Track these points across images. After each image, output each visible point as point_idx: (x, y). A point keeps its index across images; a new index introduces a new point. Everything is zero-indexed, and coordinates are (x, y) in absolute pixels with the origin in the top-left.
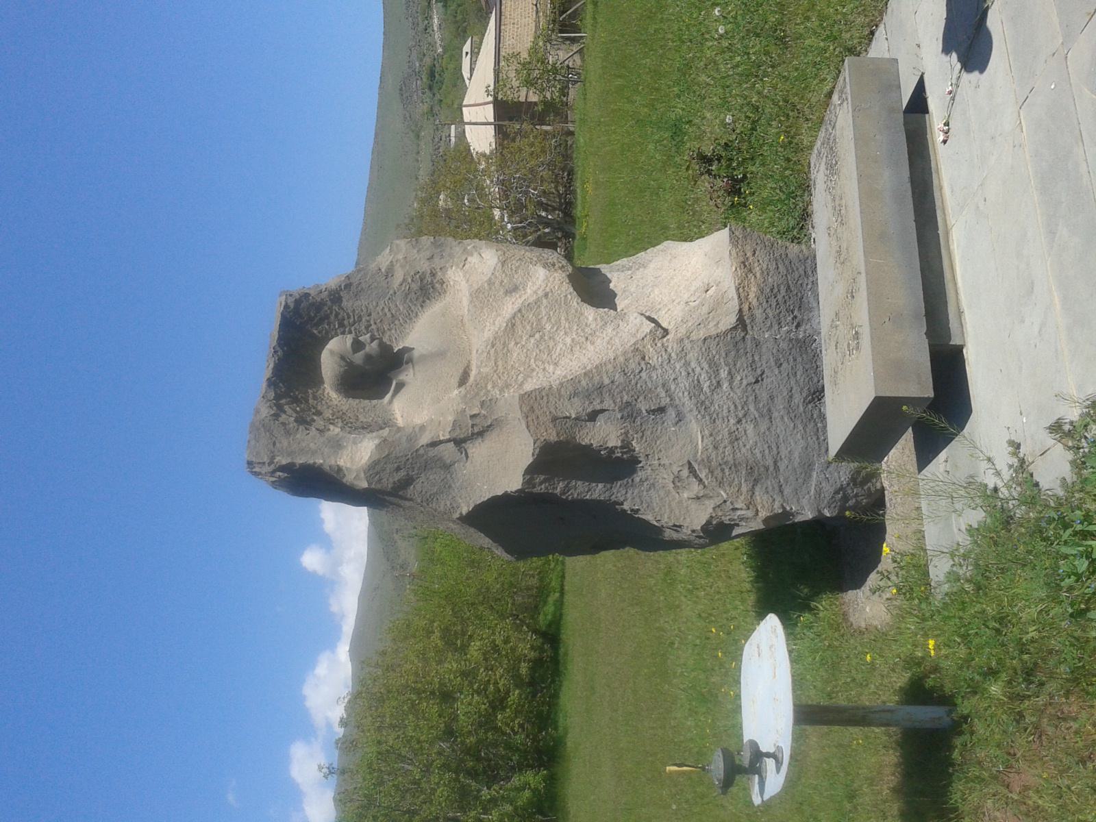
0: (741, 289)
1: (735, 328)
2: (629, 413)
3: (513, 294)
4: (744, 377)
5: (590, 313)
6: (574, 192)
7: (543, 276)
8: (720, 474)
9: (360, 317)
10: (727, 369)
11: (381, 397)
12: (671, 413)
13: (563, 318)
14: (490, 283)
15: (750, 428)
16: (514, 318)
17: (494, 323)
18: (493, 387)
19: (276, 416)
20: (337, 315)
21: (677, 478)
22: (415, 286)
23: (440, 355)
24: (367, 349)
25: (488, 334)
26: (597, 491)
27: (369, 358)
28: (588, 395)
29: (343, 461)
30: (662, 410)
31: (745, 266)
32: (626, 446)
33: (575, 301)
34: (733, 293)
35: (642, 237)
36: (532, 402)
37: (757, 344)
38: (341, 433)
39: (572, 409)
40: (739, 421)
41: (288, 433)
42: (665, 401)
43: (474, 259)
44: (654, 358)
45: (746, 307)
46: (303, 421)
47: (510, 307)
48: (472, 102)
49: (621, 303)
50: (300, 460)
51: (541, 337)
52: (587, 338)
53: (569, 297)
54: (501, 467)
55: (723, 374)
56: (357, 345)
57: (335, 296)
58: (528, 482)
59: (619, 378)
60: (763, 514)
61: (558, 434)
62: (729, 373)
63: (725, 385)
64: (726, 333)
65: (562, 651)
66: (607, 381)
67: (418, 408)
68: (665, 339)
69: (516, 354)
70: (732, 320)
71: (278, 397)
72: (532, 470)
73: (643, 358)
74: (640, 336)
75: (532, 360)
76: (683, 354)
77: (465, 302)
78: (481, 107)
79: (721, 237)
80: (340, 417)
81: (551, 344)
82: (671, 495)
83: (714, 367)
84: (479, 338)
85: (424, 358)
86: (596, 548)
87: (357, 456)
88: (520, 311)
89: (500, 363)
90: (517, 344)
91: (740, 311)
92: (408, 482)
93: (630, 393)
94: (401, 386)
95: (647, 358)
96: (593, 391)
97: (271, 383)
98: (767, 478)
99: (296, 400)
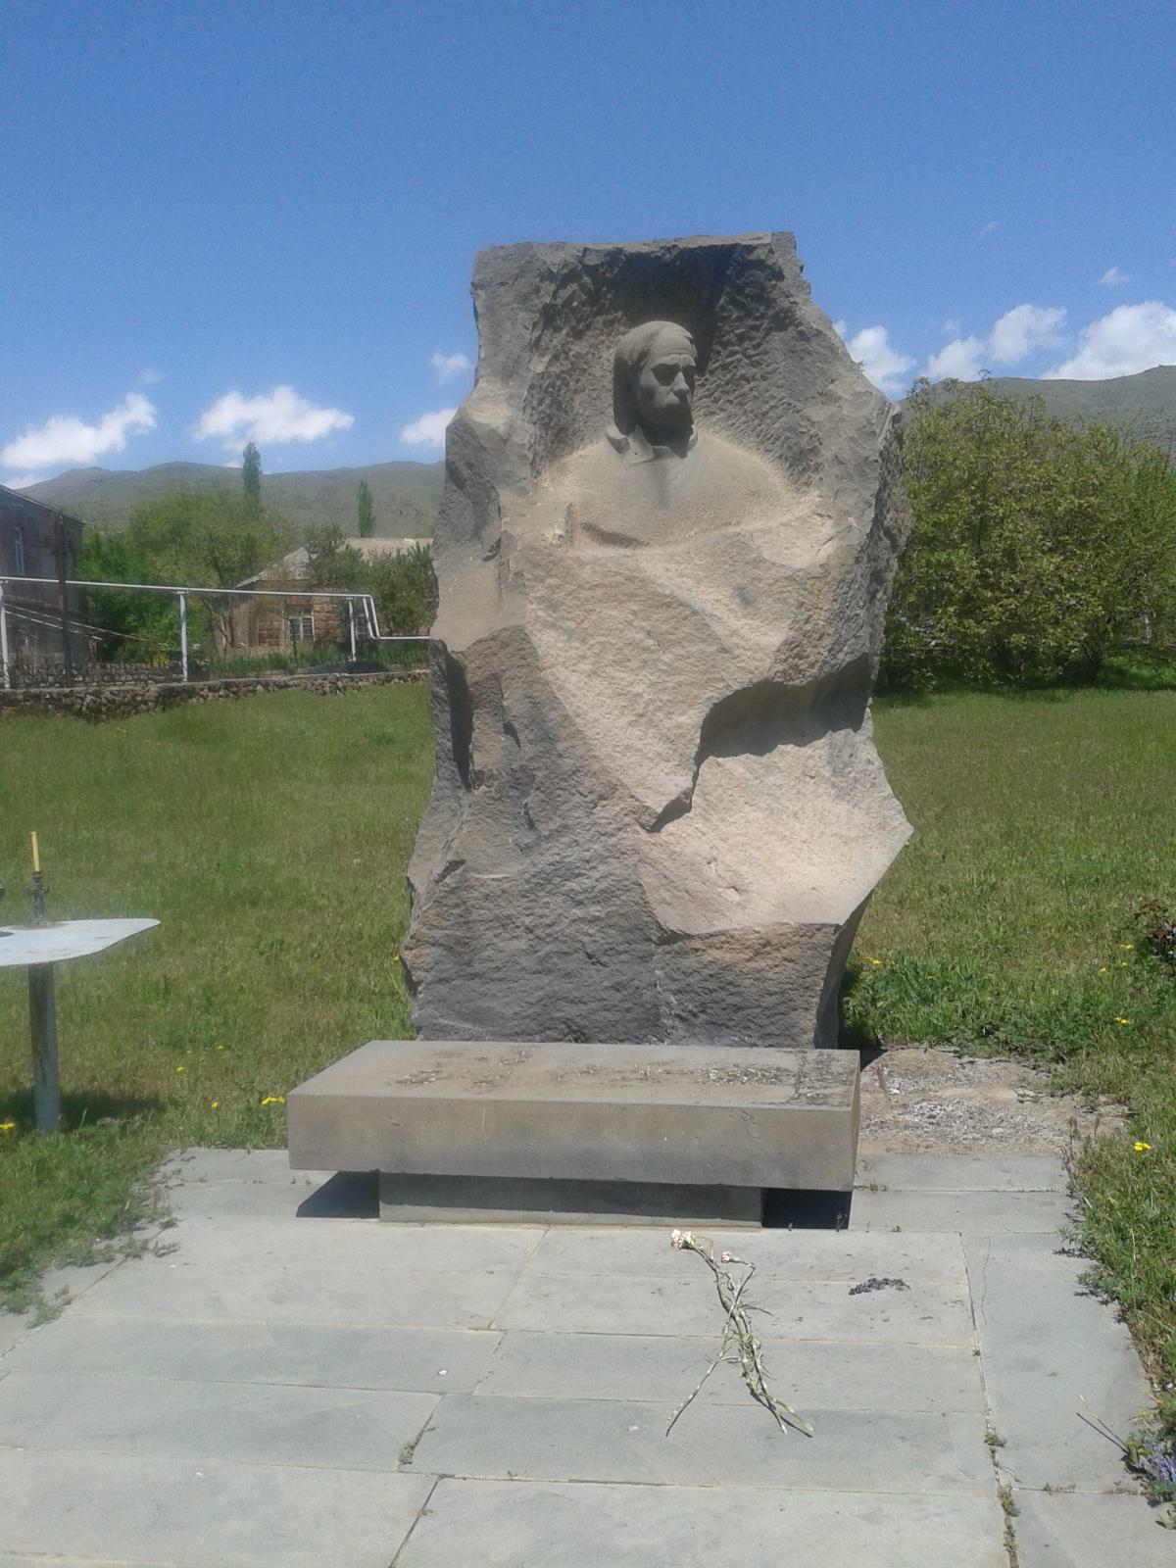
0: (724, 939)
1: (661, 928)
2: (520, 780)
3: (738, 600)
4: (594, 938)
5: (691, 719)
8: (450, 903)
9: (757, 364)
10: (602, 915)
12: (528, 838)
13: (682, 678)
14: (758, 562)
15: (521, 944)
16: (681, 605)
18: (550, 587)
19: (550, 276)
20: (756, 328)
22: (804, 441)
24: (663, 389)
27: (650, 393)
28: (536, 721)
30: (531, 825)
31: (764, 946)
33: (714, 694)
34: (720, 925)
37: (644, 958)
38: (531, 375)
39: (513, 700)
40: (529, 930)
41: (524, 299)
42: (544, 829)
44: (604, 813)
45: (697, 944)
46: (549, 317)
51: (646, 649)
52: (641, 715)
53: (722, 685)
55: (594, 910)
57: (784, 320)
59: (568, 763)
61: (476, 683)
62: (597, 919)
63: (578, 912)
64: (650, 914)
65: (1060, 693)
66: (560, 747)
68: (639, 828)
69: (614, 614)
70: (673, 921)
71: (592, 271)
73: (602, 797)
74: (640, 792)
75: (603, 639)
81: (634, 664)
83: (605, 897)
88: (695, 613)
89: (598, 592)
90: (634, 613)
91: (690, 937)
95: (604, 802)
96: (544, 726)
97: (614, 256)
98: (455, 963)
99: (594, 298)
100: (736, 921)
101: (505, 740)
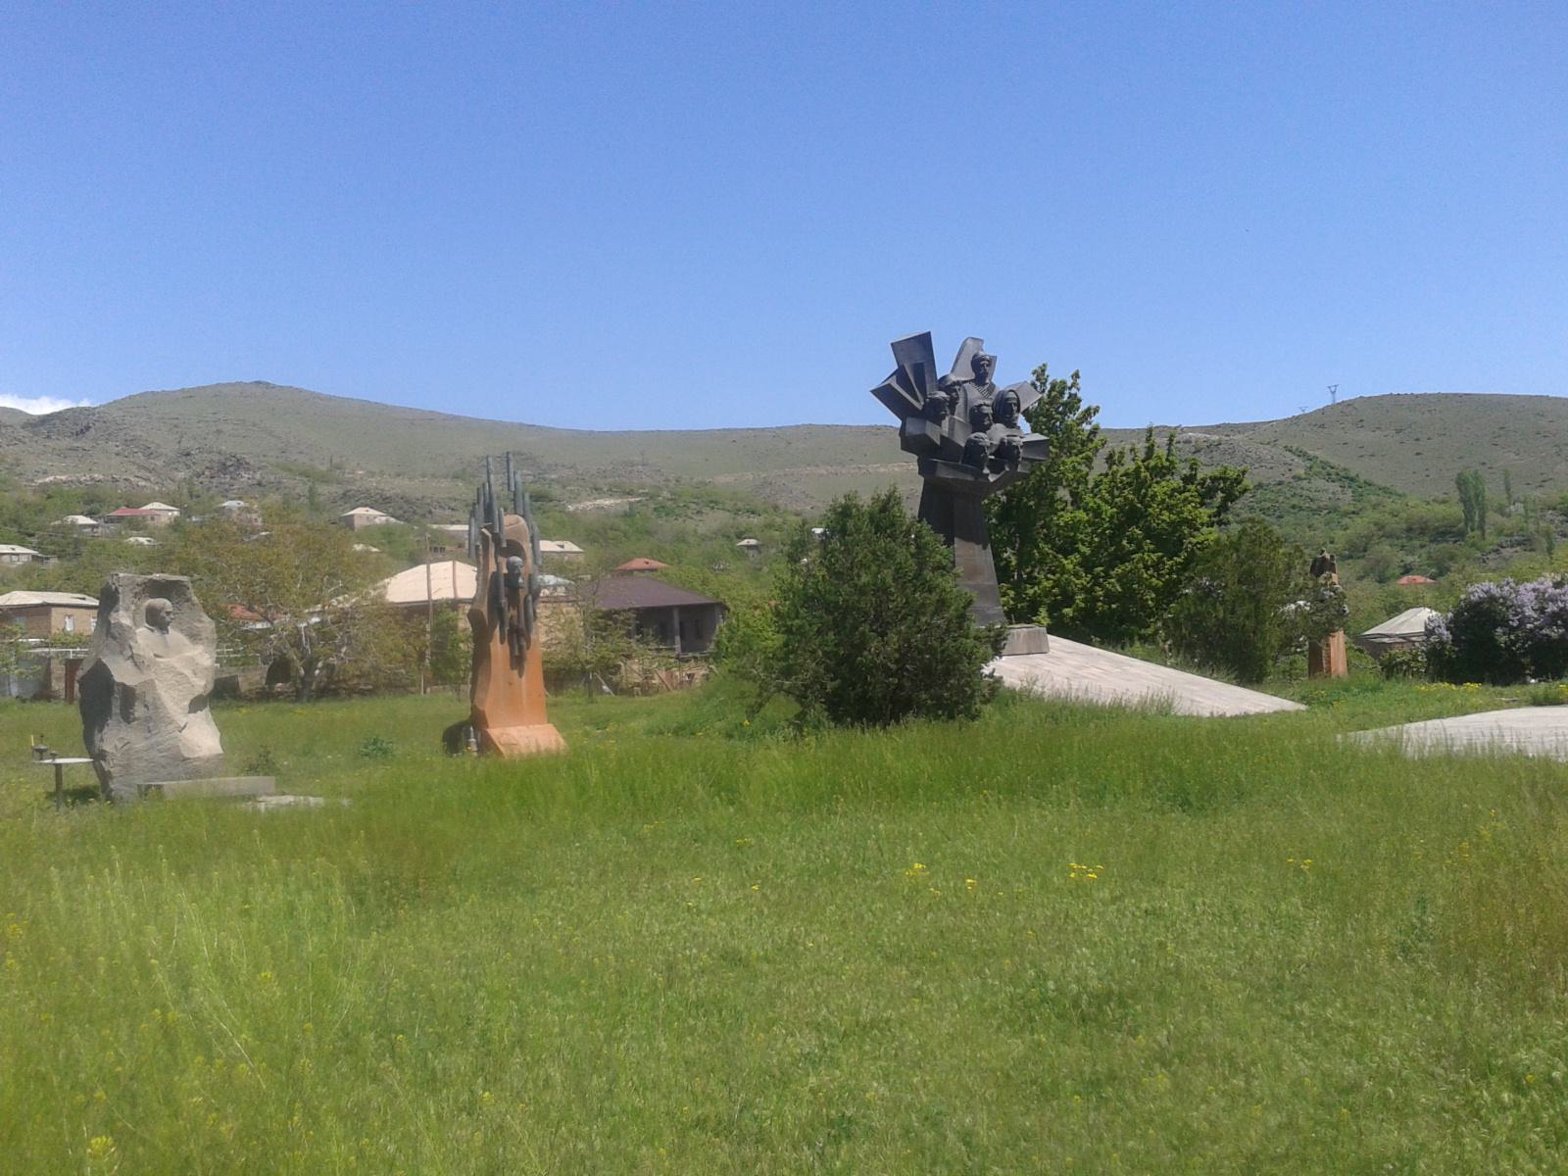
2: (148, 719)
4: (163, 761)
5: (187, 703)
7: (201, 684)
11: (147, 622)
15: (144, 764)
17: (179, 667)
21: (123, 738)
23: (166, 645)
25: (176, 665)
26: (116, 709)
31: (208, 760)
32: (135, 719)
33: (192, 697)
35: (222, 727)
39: (149, 699)
43: (207, 656)
44: (170, 727)
47: (188, 672)
48: (457, 572)
49: (191, 715)
50: (121, 596)
54: (122, 673)
56: (168, 613)
67: (144, 638)
70: (186, 756)
72: (123, 685)
76: (171, 738)
77: (187, 654)
78: (451, 584)
79: (221, 751)
80: (138, 607)
82: (113, 738)
84: (172, 661)
86: (84, 714)
87: (122, 617)
92: (114, 638)
93: (156, 718)
94: (152, 631)
96: (156, 706)
100: (201, 754)
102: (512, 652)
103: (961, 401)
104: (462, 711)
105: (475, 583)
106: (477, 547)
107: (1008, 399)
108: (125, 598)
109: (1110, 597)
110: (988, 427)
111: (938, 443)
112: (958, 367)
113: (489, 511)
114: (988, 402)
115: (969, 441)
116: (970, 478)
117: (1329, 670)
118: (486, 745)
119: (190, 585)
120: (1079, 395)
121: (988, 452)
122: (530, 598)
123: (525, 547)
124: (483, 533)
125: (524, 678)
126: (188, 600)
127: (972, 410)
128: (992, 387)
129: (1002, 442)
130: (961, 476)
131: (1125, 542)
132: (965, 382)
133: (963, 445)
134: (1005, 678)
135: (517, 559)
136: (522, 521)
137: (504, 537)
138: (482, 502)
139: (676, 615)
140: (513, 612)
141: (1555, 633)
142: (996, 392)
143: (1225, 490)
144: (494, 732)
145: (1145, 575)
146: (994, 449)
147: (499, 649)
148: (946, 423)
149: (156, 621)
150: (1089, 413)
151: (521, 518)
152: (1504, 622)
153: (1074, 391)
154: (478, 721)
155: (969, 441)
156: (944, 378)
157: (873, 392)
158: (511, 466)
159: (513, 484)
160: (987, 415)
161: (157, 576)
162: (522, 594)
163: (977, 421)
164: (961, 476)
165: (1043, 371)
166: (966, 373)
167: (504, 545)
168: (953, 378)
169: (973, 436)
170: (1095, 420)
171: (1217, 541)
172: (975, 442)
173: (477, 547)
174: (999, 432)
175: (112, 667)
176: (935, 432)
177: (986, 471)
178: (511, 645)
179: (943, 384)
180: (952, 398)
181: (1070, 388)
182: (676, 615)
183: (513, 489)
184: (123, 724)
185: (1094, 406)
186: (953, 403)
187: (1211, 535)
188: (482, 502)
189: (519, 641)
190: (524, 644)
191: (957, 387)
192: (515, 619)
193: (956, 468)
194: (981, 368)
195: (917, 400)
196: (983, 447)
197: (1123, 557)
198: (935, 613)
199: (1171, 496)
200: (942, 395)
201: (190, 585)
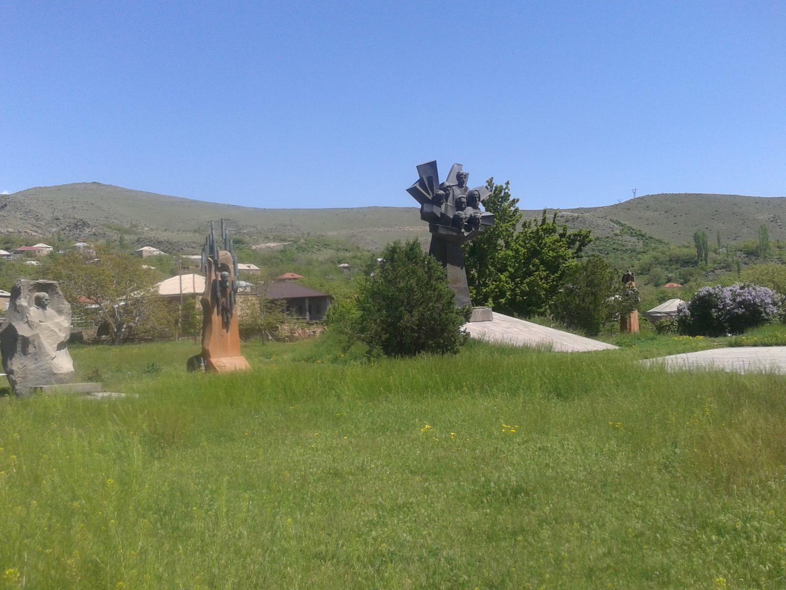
0: (60, 374)
2: (35, 354)
4: (44, 375)
5: (56, 346)
6: (140, 342)
7: (63, 336)
12: (35, 362)
23: (45, 316)
25: (50, 326)
26: (19, 349)
29: (22, 299)
30: (36, 360)
31: (66, 374)
32: (29, 354)
33: (59, 342)
35: (74, 358)
36: (37, 336)
41: (27, 288)
43: (67, 321)
47: (56, 330)
48: (195, 280)
49: (58, 352)
50: (22, 291)
54: (23, 330)
56: (46, 300)
58: (20, 336)
60: (17, 380)
67: (34, 312)
72: (23, 336)
76: (48, 363)
77: (57, 321)
79: (73, 370)
80: (31, 297)
82: (16, 364)
84: (49, 324)
85: (44, 313)
87: (23, 302)
92: (19, 312)
93: (40, 353)
94: (38, 309)
96: (40, 347)
100: (62, 372)
101: (34, 348)
102: (223, 319)
103: (451, 196)
104: (197, 350)
105: (204, 285)
106: (206, 267)
107: (474, 195)
108: (24, 292)
109: (523, 293)
110: (464, 209)
111: (439, 216)
112: (449, 179)
113: (212, 249)
114: (464, 196)
115: (455, 216)
116: (455, 234)
117: (630, 330)
118: (209, 366)
119: (58, 285)
120: (509, 193)
121: (464, 221)
122: (233, 292)
123: (230, 267)
124: (208, 260)
125: (229, 333)
126: (57, 293)
127: (456, 200)
128: (466, 189)
129: (471, 215)
130: (450, 233)
131: (531, 266)
132: (453, 186)
133: (452, 217)
134: (471, 334)
135: (226, 273)
136: (229, 254)
137: (220, 262)
138: (208, 244)
139: (307, 301)
140: (224, 300)
141: (740, 311)
142: (468, 191)
143: (580, 241)
144: (214, 360)
145: (540, 283)
146: (467, 220)
147: (216, 318)
148: (443, 206)
149: (40, 303)
150: (514, 201)
151: (228, 253)
152: (716, 306)
153: (506, 191)
154: (205, 355)
155: (455, 216)
156: (443, 184)
157: (407, 190)
158: (224, 226)
159: (224, 235)
160: (464, 202)
161: (41, 281)
162: (229, 290)
163: (459, 205)
164: (450, 233)
165: (491, 181)
166: (453, 182)
167: (220, 266)
168: (447, 184)
169: (456, 213)
170: (517, 205)
171: (576, 266)
172: (458, 216)
173: (206, 267)
174: (469, 211)
175: (17, 327)
176: (438, 211)
177: (463, 230)
178: (222, 316)
179: (442, 187)
180: (446, 194)
181: (505, 190)
182: (307, 301)
183: (224, 238)
184: (23, 356)
185: (516, 198)
186: (447, 196)
187: (573, 262)
188: (208, 244)
189: (226, 314)
190: (229, 316)
191: (449, 189)
192: (225, 304)
193: (447, 228)
194: (461, 179)
195: (429, 195)
196: (462, 219)
197: (530, 274)
198: (437, 301)
199: (553, 244)
200: (441, 192)
201: (58, 285)
